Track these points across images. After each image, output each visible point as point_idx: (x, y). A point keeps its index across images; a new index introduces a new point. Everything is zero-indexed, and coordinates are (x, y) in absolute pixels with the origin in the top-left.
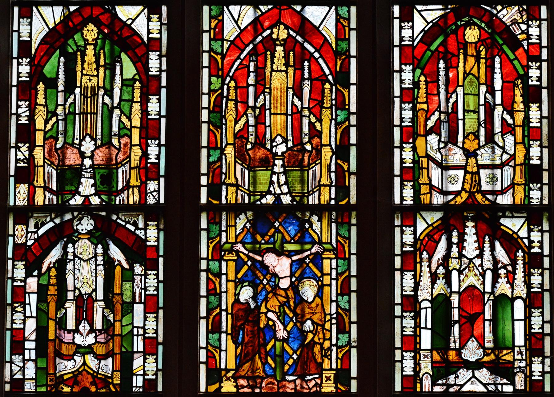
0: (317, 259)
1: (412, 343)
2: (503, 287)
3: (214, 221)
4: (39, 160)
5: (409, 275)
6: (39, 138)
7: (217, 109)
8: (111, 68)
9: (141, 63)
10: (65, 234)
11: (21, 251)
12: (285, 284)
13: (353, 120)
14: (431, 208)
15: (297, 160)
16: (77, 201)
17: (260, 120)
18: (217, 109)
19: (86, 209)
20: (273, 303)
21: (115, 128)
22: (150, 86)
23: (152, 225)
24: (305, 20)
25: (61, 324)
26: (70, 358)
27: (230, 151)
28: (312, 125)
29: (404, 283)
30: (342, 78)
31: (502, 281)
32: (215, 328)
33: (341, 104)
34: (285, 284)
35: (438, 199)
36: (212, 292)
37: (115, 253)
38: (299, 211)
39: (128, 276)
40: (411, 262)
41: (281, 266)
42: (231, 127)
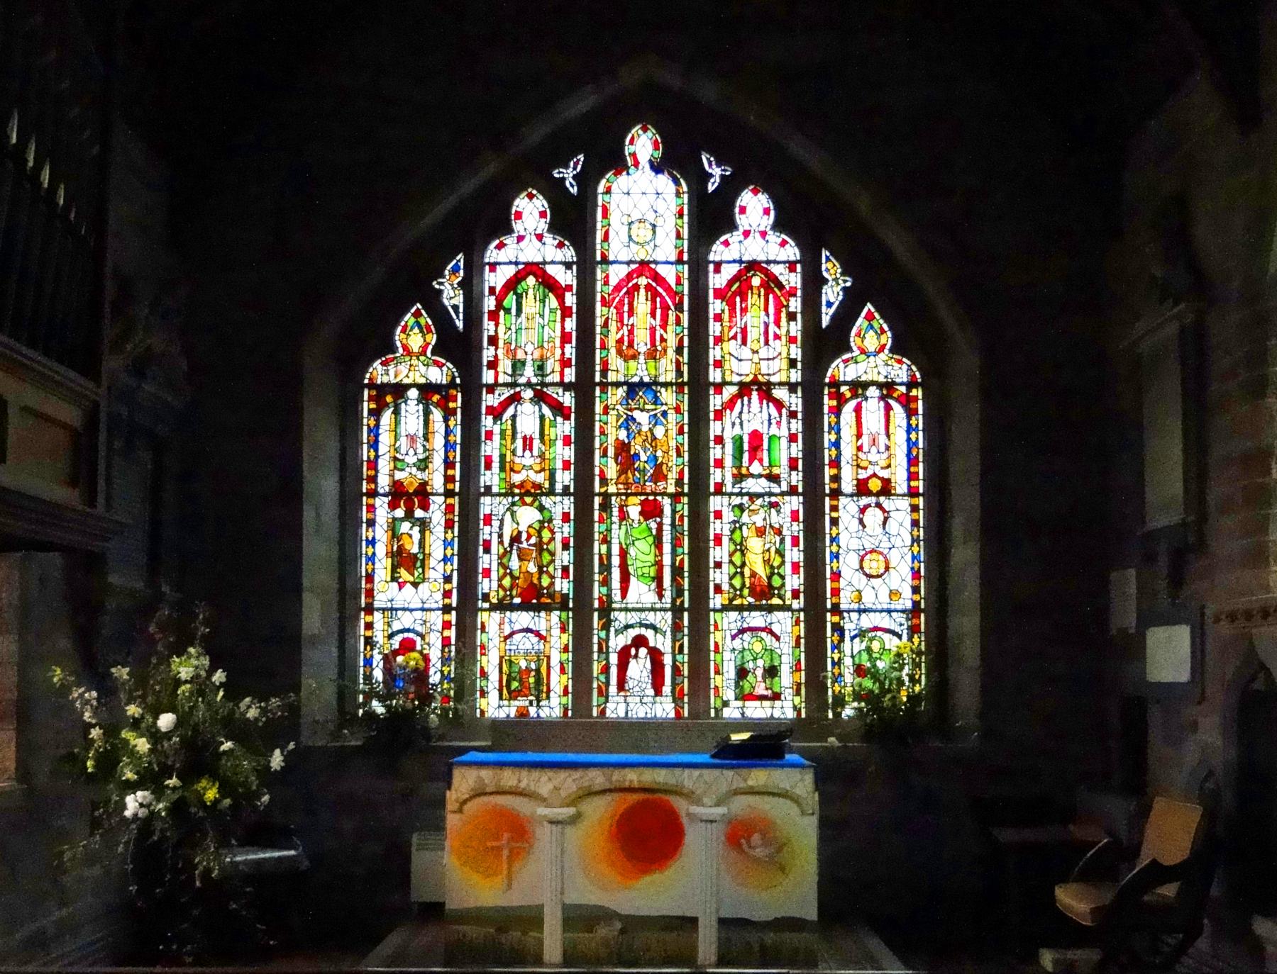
0: (664, 414)
1: (719, 463)
2: (774, 430)
3: (604, 391)
4: (501, 356)
5: (718, 423)
6: (501, 343)
7: (606, 325)
8: (543, 301)
9: (561, 299)
10: (516, 399)
11: (490, 410)
12: (645, 428)
13: (686, 332)
14: (731, 384)
15: (652, 355)
16: (522, 380)
17: (631, 332)
18: (606, 325)
19: (529, 384)
20: (639, 440)
21: (546, 339)
22: (566, 312)
23: (567, 394)
24: (657, 273)
25: (514, 452)
26: (518, 472)
27: (613, 351)
28: (661, 336)
29: (715, 428)
30: (679, 307)
31: (774, 426)
32: (605, 454)
33: (678, 322)
34: (645, 428)
35: (736, 379)
36: (603, 433)
37: (546, 411)
38: (652, 386)
39: (553, 424)
40: (719, 415)
41: (642, 417)
42: (613, 337)
